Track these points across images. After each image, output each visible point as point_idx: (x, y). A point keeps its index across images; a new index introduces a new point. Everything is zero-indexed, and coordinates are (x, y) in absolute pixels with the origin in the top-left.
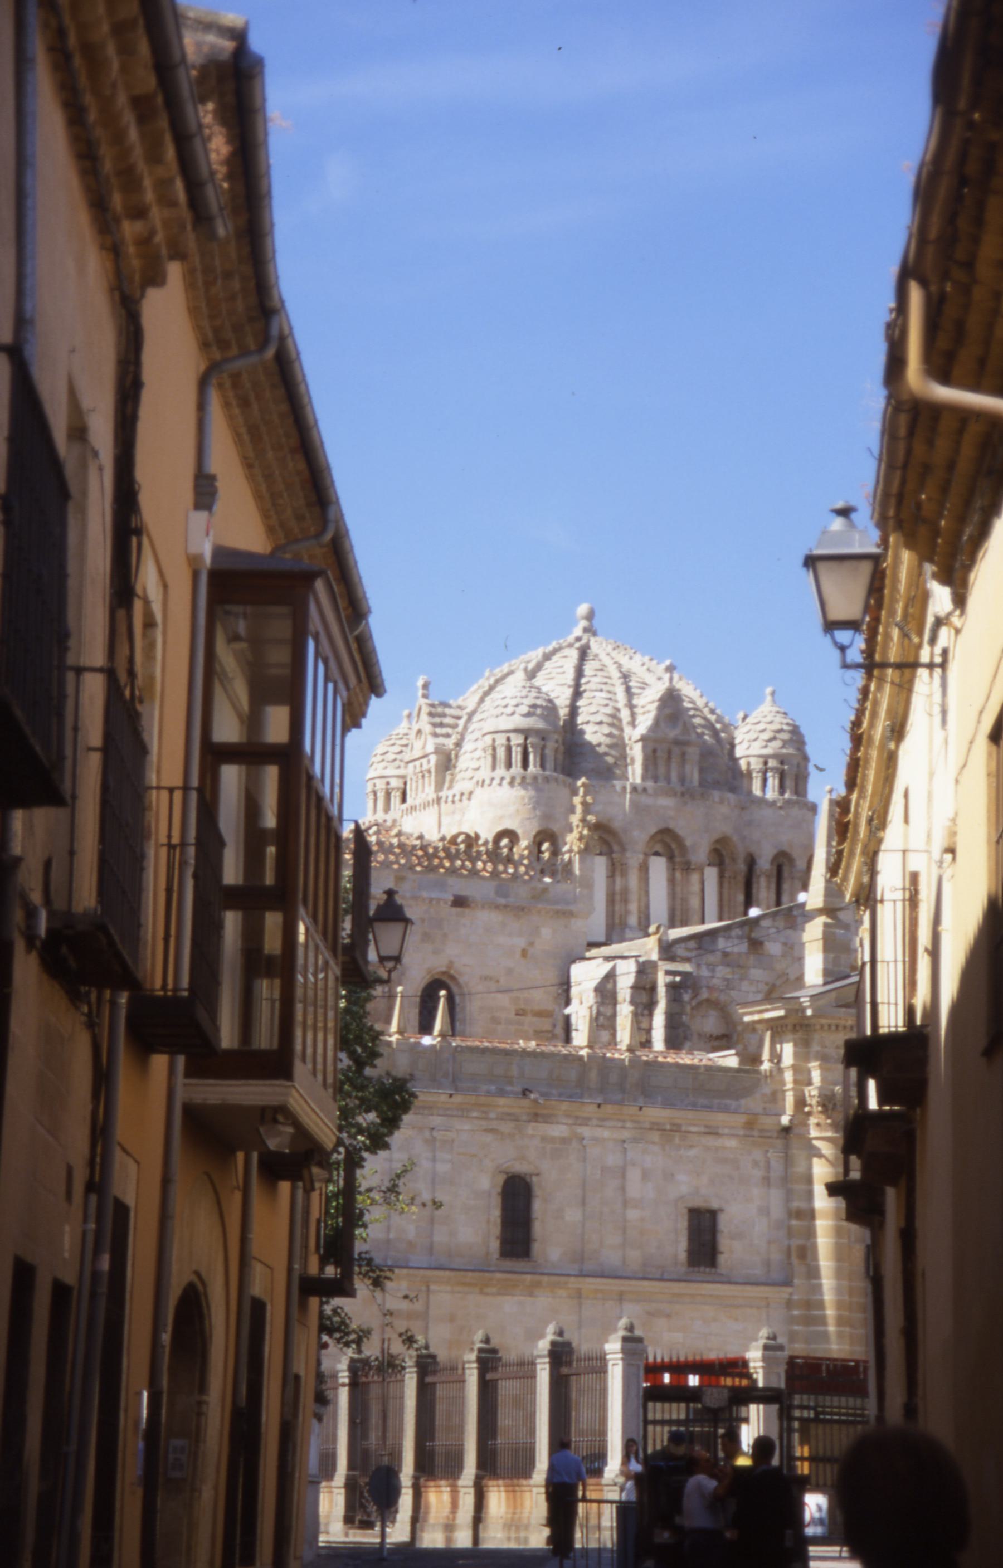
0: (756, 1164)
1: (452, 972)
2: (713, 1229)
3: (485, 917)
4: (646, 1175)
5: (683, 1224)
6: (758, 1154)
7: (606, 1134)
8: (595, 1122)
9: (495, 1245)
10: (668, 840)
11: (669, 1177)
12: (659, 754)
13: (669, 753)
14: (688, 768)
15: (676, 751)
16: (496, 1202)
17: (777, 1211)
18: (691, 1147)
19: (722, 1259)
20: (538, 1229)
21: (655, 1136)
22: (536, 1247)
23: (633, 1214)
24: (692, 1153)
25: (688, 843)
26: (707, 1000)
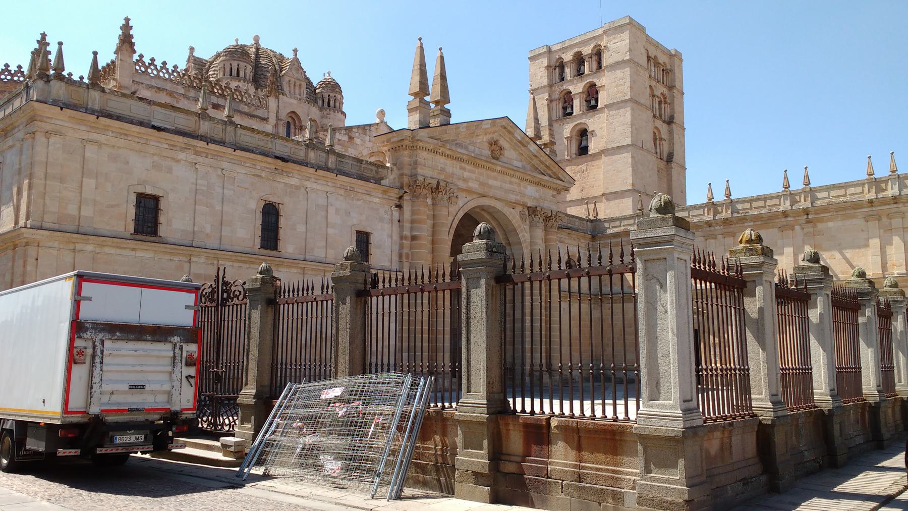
0: (386, 213)
2: (367, 242)
4: (337, 211)
5: (354, 238)
7: (319, 187)
8: (313, 180)
11: (348, 214)
15: (298, 83)
16: (259, 216)
18: (358, 200)
19: (371, 257)
20: (282, 233)
21: (342, 192)
22: (281, 245)
23: (331, 231)
24: (359, 203)
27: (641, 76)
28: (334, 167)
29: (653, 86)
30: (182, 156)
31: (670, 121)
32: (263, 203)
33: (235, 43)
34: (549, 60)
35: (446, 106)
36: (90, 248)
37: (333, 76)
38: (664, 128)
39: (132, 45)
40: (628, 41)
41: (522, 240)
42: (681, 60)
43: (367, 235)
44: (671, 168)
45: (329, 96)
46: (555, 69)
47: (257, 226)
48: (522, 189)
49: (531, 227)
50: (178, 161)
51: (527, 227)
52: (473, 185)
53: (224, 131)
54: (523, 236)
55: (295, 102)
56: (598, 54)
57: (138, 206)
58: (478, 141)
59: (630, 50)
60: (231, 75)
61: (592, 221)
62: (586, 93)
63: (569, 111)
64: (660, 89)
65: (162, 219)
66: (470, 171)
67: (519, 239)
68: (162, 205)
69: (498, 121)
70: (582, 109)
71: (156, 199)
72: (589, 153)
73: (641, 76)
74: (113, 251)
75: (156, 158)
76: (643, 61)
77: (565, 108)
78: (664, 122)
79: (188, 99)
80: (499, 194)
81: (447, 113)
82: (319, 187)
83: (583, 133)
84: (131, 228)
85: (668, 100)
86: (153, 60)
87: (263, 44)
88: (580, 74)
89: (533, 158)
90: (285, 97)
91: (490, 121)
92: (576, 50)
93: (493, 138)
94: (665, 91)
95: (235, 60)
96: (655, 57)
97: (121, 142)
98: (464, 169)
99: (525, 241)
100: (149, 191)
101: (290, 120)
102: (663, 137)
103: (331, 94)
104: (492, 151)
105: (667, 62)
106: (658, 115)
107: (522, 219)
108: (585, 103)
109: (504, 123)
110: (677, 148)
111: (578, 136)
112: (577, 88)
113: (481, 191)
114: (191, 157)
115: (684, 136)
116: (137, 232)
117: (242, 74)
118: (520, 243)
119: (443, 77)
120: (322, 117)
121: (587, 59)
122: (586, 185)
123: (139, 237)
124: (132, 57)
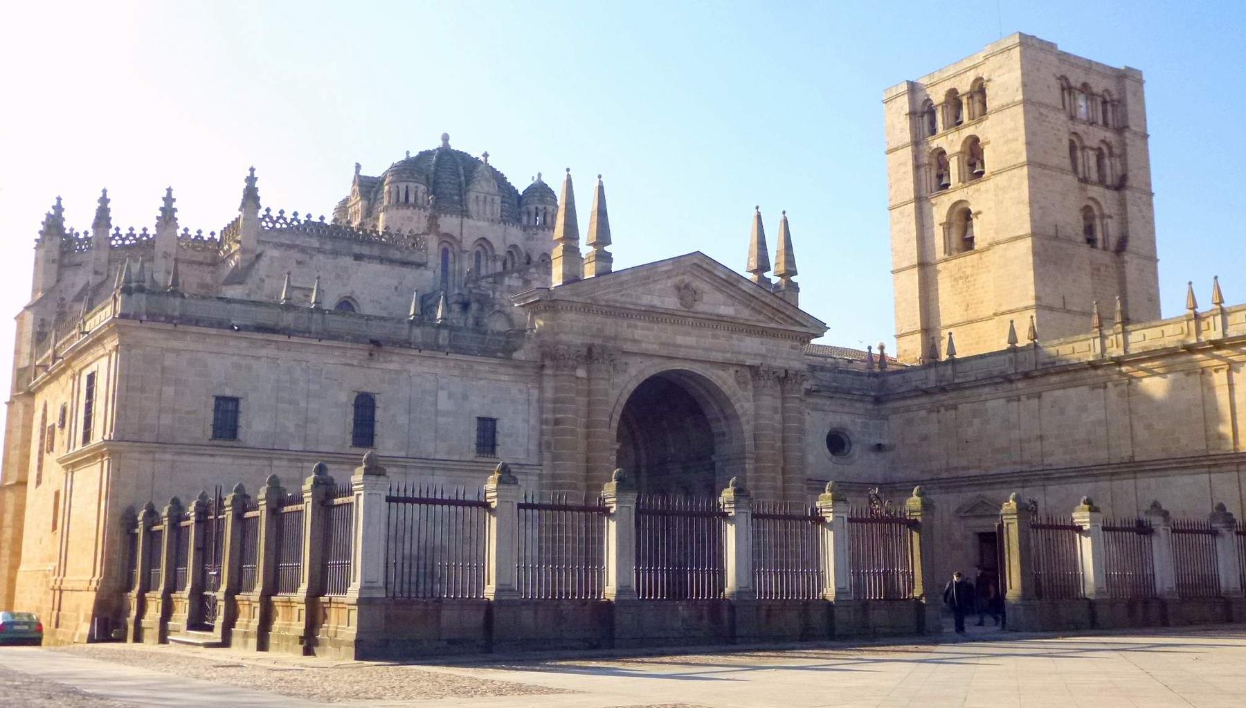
0: (521, 391)
1: (354, 297)
3: (375, 267)
4: (450, 396)
6: (522, 386)
7: (425, 369)
9: (349, 437)
10: (484, 244)
11: (465, 397)
12: (480, 199)
13: (485, 198)
14: (496, 206)
15: (489, 199)
16: (351, 411)
17: (533, 421)
18: (481, 379)
19: (498, 449)
20: (378, 428)
22: (376, 440)
23: (442, 420)
25: (494, 246)
26: (499, 311)
27: (1049, 122)
28: (447, 342)
29: (1080, 133)
30: (263, 352)
31: (1121, 185)
32: (356, 394)
33: (403, 157)
34: (912, 101)
35: (607, 249)
36: (168, 457)
37: (545, 179)
38: (1106, 199)
39: (258, 198)
40: (1019, 73)
41: (740, 412)
42: (1140, 82)
43: (493, 421)
44: (1123, 262)
45: (537, 208)
46: (922, 116)
47: (348, 421)
48: (735, 342)
49: (754, 396)
50: (258, 358)
51: (750, 394)
52: (653, 347)
53: (310, 319)
54: (742, 407)
55: (485, 224)
56: (979, 90)
57: (217, 409)
58: (659, 287)
59: (1024, 85)
60: (398, 200)
61: (876, 375)
62: (968, 151)
63: (945, 182)
64: (1095, 136)
65: (242, 421)
66: (643, 328)
67: (735, 411)
68: (242, 404)
69: (682, 259)
70: (962, 179)
71: (235, 400)
72: (976, 247)
73: (1049, 122)
74: (192, 459)
75: (235, 358)
76: (1053, 95)
77: (940, 177)
78: (1107, 187)
79: (324, 253)
80: (692, 354)
81: (608, 258)
82: (425, 369)
83: (963, 216)
84: (210, 433)
85: (1116, 151)
86: (282, 212)
87: (455, 145)
88: (957, 123)
89: (752, 299)
90: (471, 222)
91: (671, 262)
92: (948, 86)
93: (683, 281)
94: (1109, 136)
95: (401, 181)
96: (1085, 85)
97: (200, 347)
98: (636, 327)
99: (744, 414)
100: (228, 392)
101: (479, 248)
102: (1106, 211)
103: (540, 207)
104: (681, 298)
105: (1113, 89)
106: (1094, 176)
107: (739, 383)
108: (967, 168)
109: (695, 261)
110: (1135, 228)
111: (960, 221)
112: (950, 142)
113: (664, 352)
114: (270, 351)
115: (1150, 205)
116: (215, 437)
117: (412, 199)
118: (736, 417)
119: (602, 213)
120: (527, 239)
121: (965, 100)
122: (973, 299)
123: (216, 442)
124: (256, 213)
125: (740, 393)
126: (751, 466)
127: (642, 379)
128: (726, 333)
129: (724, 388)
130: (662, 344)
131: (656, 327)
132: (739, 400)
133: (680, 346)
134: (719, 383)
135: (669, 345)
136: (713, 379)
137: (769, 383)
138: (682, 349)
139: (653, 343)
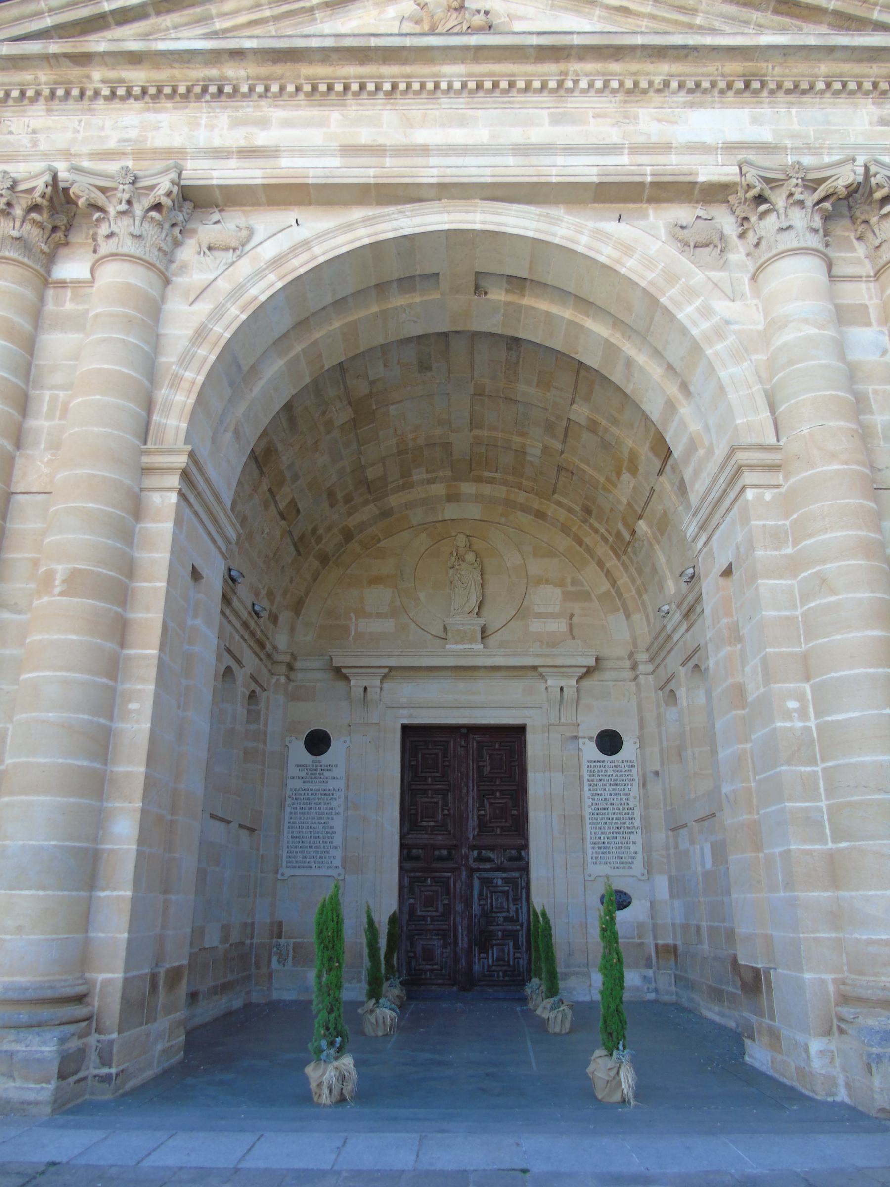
49: (754, 278)
54: (706, 312)
66: (287, 123)
98: (264, 123)
125: (699, 277)
126: (768, 495)
127: (300, 265)
128: (609, 104)
129: (629, 267)
130: (349, 150)
131: (335, 116)
132: (691, 293)
133: (424, 150)
134: (605, 254)
135: (377, 150)
136: (582, 244)
137: (798, 218)
138: (433, 161)
139: (322, 152)
